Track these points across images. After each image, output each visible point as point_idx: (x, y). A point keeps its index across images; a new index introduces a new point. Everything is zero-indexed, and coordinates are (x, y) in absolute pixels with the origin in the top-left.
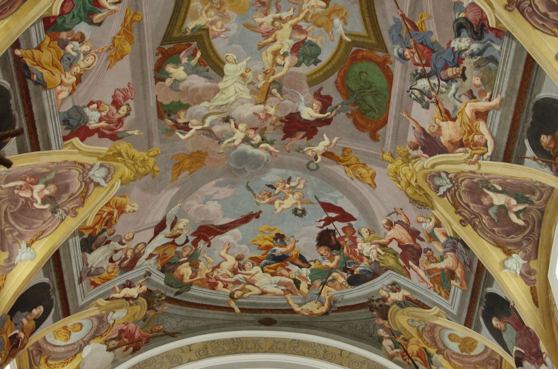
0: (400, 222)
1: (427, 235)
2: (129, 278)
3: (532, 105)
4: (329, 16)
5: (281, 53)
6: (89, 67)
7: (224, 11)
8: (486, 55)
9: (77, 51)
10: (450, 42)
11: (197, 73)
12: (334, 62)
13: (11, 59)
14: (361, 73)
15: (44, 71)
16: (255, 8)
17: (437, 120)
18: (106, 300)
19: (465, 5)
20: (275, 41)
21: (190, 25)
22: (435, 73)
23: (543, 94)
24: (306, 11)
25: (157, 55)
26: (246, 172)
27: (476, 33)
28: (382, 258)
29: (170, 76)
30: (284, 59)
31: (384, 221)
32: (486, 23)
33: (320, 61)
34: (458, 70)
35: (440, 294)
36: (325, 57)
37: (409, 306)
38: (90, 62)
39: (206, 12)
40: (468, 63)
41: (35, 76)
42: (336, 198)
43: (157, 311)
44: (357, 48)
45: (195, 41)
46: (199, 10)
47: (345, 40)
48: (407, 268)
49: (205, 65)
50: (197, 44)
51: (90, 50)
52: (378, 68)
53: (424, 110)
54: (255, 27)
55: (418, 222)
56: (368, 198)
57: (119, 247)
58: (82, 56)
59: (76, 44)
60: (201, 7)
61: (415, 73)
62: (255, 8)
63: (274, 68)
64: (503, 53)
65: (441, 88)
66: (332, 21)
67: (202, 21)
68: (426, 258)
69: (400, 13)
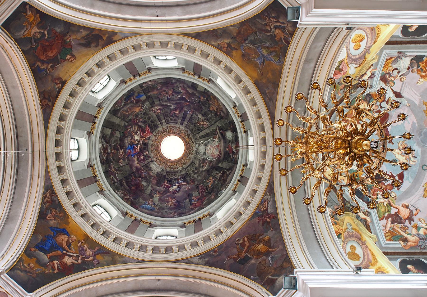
0: (411, 211)
1: (415, 225)
2: (375, 78)
18: (372, 65)
26: (419, 137)
28: (382, 205)
31: (407, 204)
35: (385, 237)
37: (361, 222)
42: (409, 179)
43: (340, 90)
48: (385, 218)
55: (419, 220)
56: (416, 194)
57: (400, 74)
68: (401, 226)
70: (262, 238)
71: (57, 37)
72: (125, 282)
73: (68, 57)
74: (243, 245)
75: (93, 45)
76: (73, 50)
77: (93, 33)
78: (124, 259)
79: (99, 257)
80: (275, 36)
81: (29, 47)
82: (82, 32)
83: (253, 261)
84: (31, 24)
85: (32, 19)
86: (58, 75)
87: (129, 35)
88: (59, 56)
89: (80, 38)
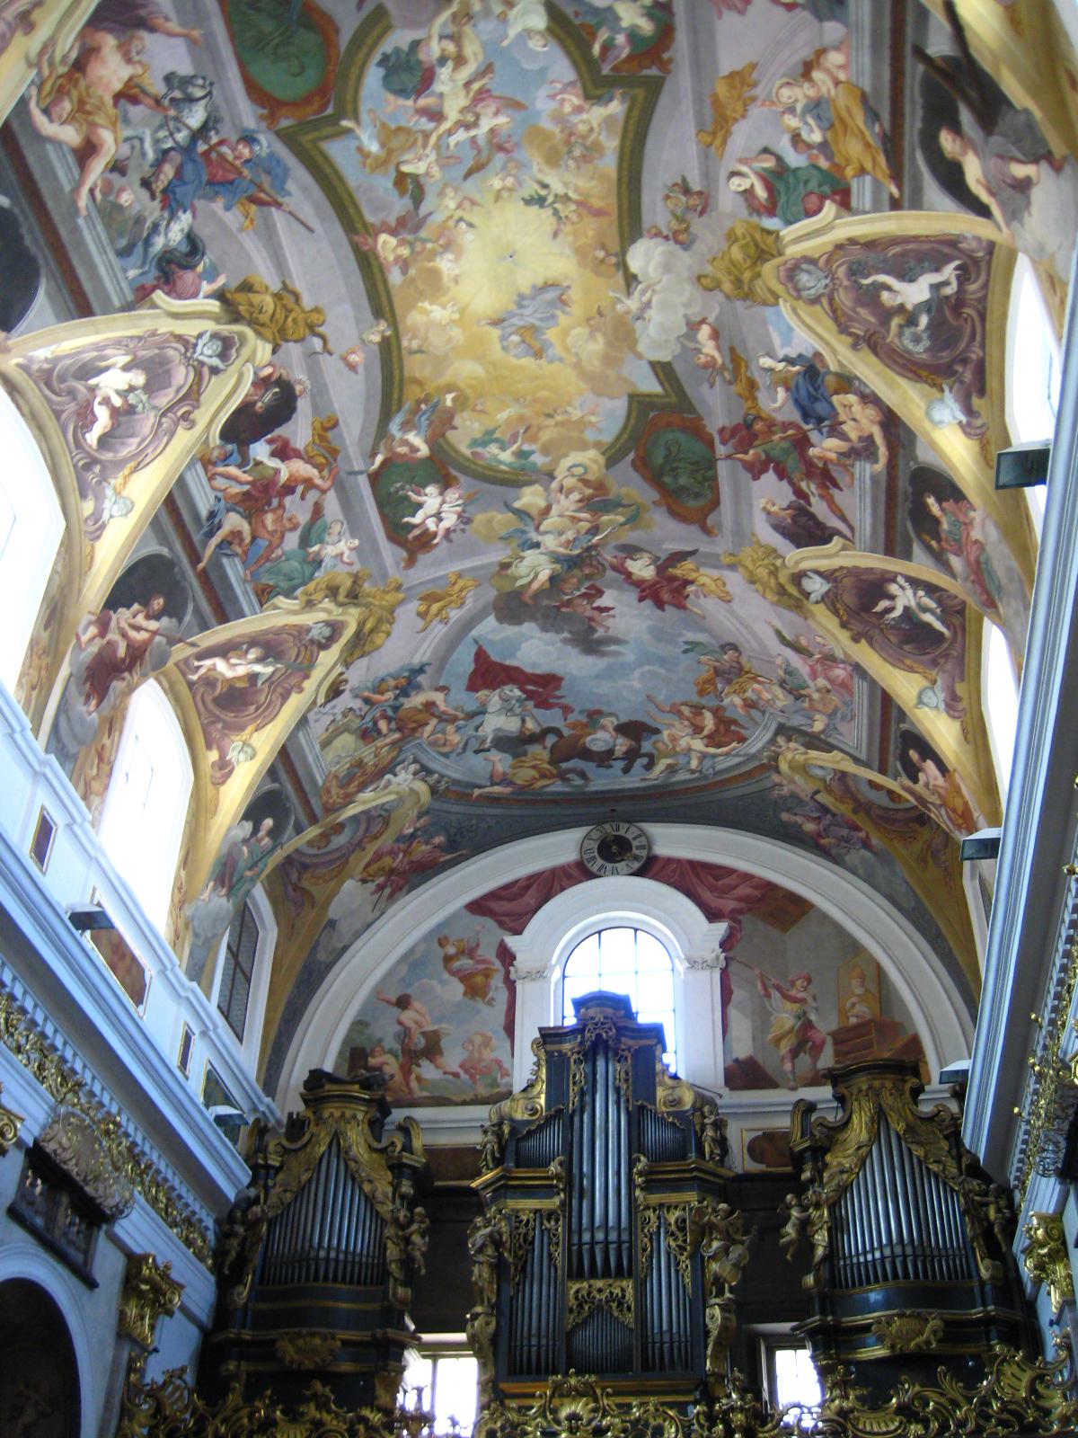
3: (41, 262)
4: (390, 152)
5: (450, 64)
6: (788, 83)
7: (562, 131)
8: (139, 249)
9: (806, 123)
10: (194, 217)
11: (596, 11)
12: (354, 72)
13: (907, 190)
14: (302, 69)
15: (862, 126)
16: (514, 140)
17: (139, 70)
19: (205, 283)
20: (467, 85)
21: (616, 107)
22: (188, 150)
23: (41, 299)
24: (428, 150)
25: (670, 61)
27: (169, 262)
29: (644, 11)
30: (443, 50)
32: (166, 289)
33: (380, 64)
34: (159, 186)
36: (373, 76)
38: (785, 92)
39: (591, 130)
40: (153, 210)
41: (877, 128)
44: (326, 113)
45: (606, 76)
46: (604, 133)
47: (349, 119)
49: (582, 26)
50: (600, 70)
51: (784, 113)
52: (279, 94)
53: (170, 68)
54: (507, 106)
58: (799, 108)
59: (805, 136)
60: (603, 138)
61: (218, 126)
62: (514, 140)
63: (455, 29)
64: (120, 275)
65: (167, 133)
66: (383, 145)
67: (597, 114)
69: (284, 207)
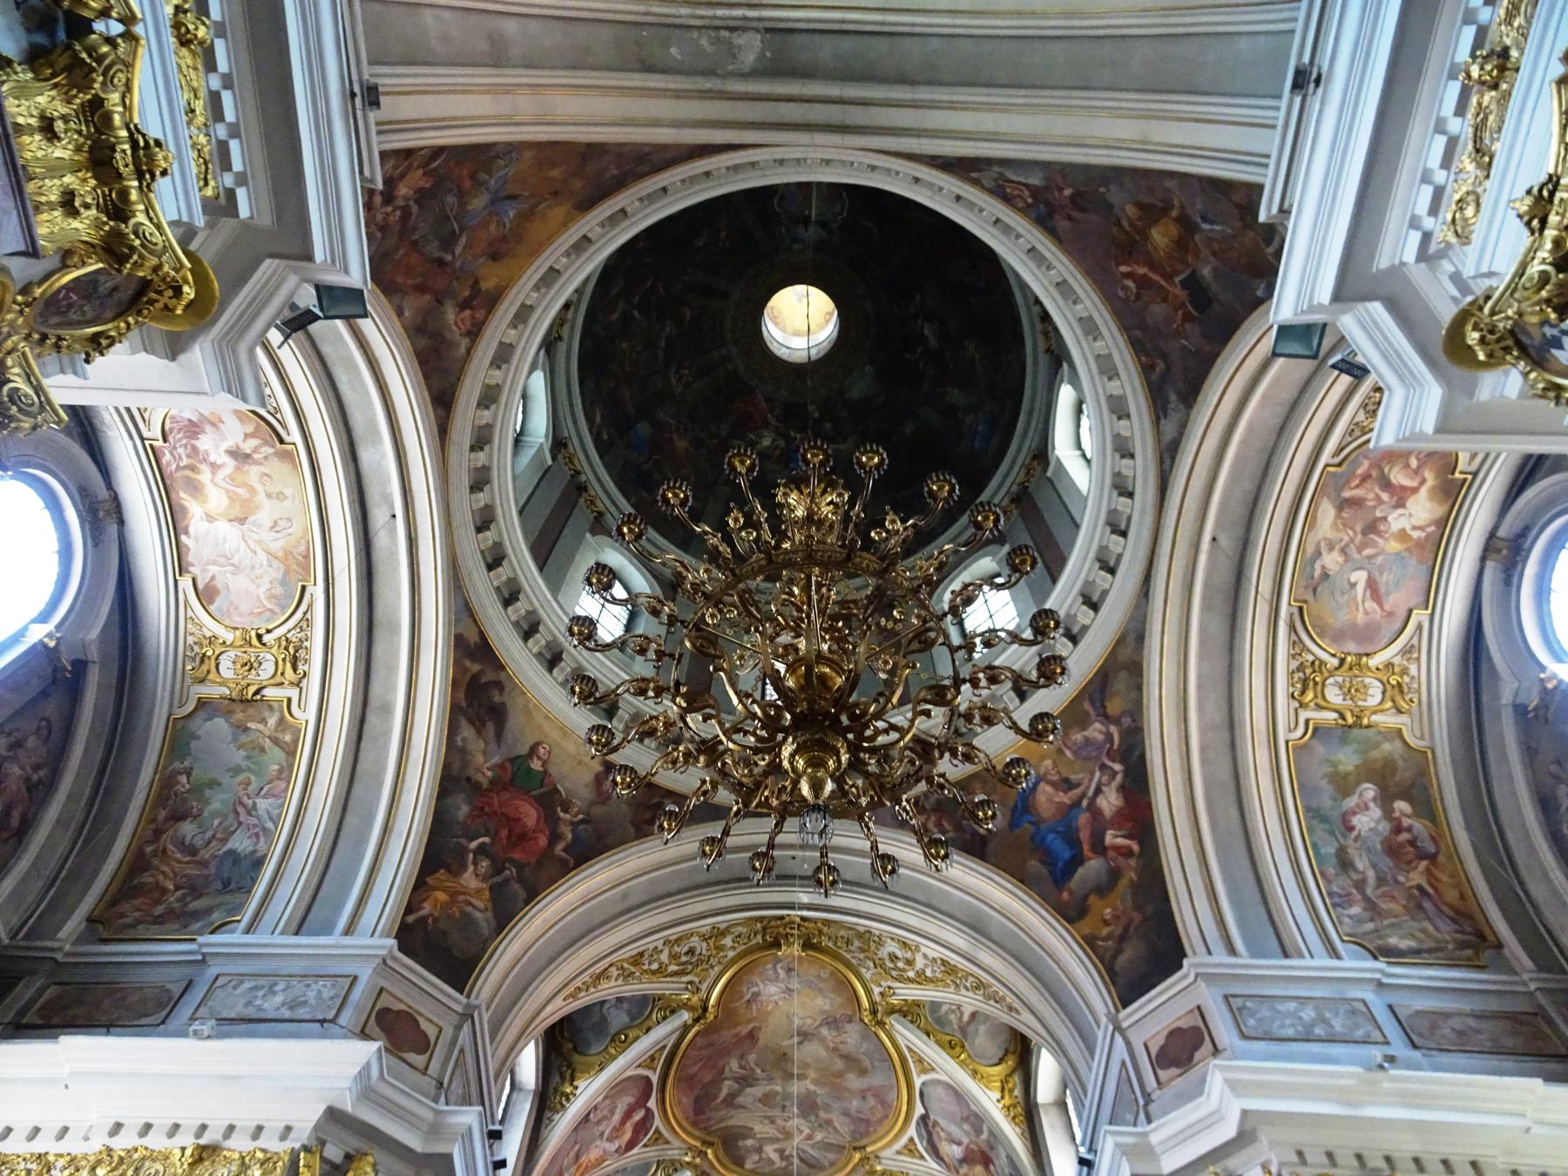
70: (1131, 224)
71: (482, 809)
72: (1203, 641)
73: (536, 765)
74: (1143, 282)
75: (497, 699)
76: (517, 753)
77: (464, 704)
78: (1131, 638)
79: (1114, 707)
80: (420, 191)
81: (517, 887)
82: (464, 739)
83: (1206, 272)
84: (453, 895)
85: (442, 896)
86: (587, 786)
87: (460, 600)
88: (534, 793)
89: (481, 742)
